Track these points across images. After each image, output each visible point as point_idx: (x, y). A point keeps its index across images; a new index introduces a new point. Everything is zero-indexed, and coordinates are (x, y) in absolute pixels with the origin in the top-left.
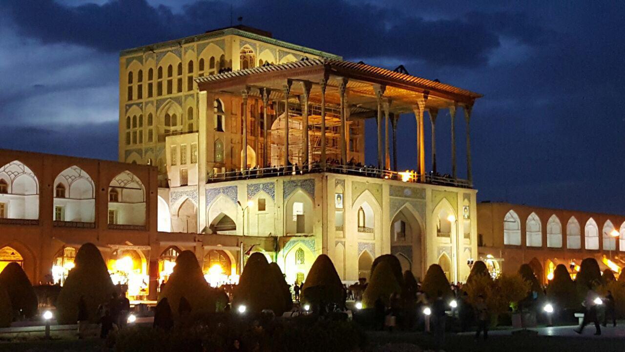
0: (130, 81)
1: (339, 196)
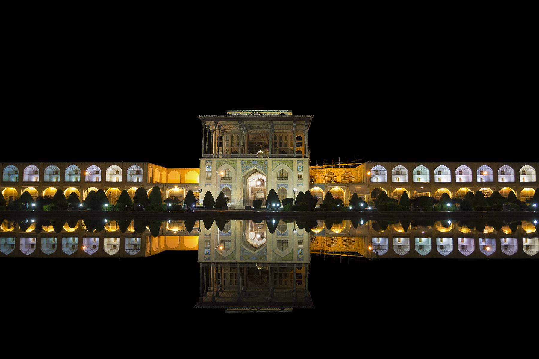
1: (209, 167)
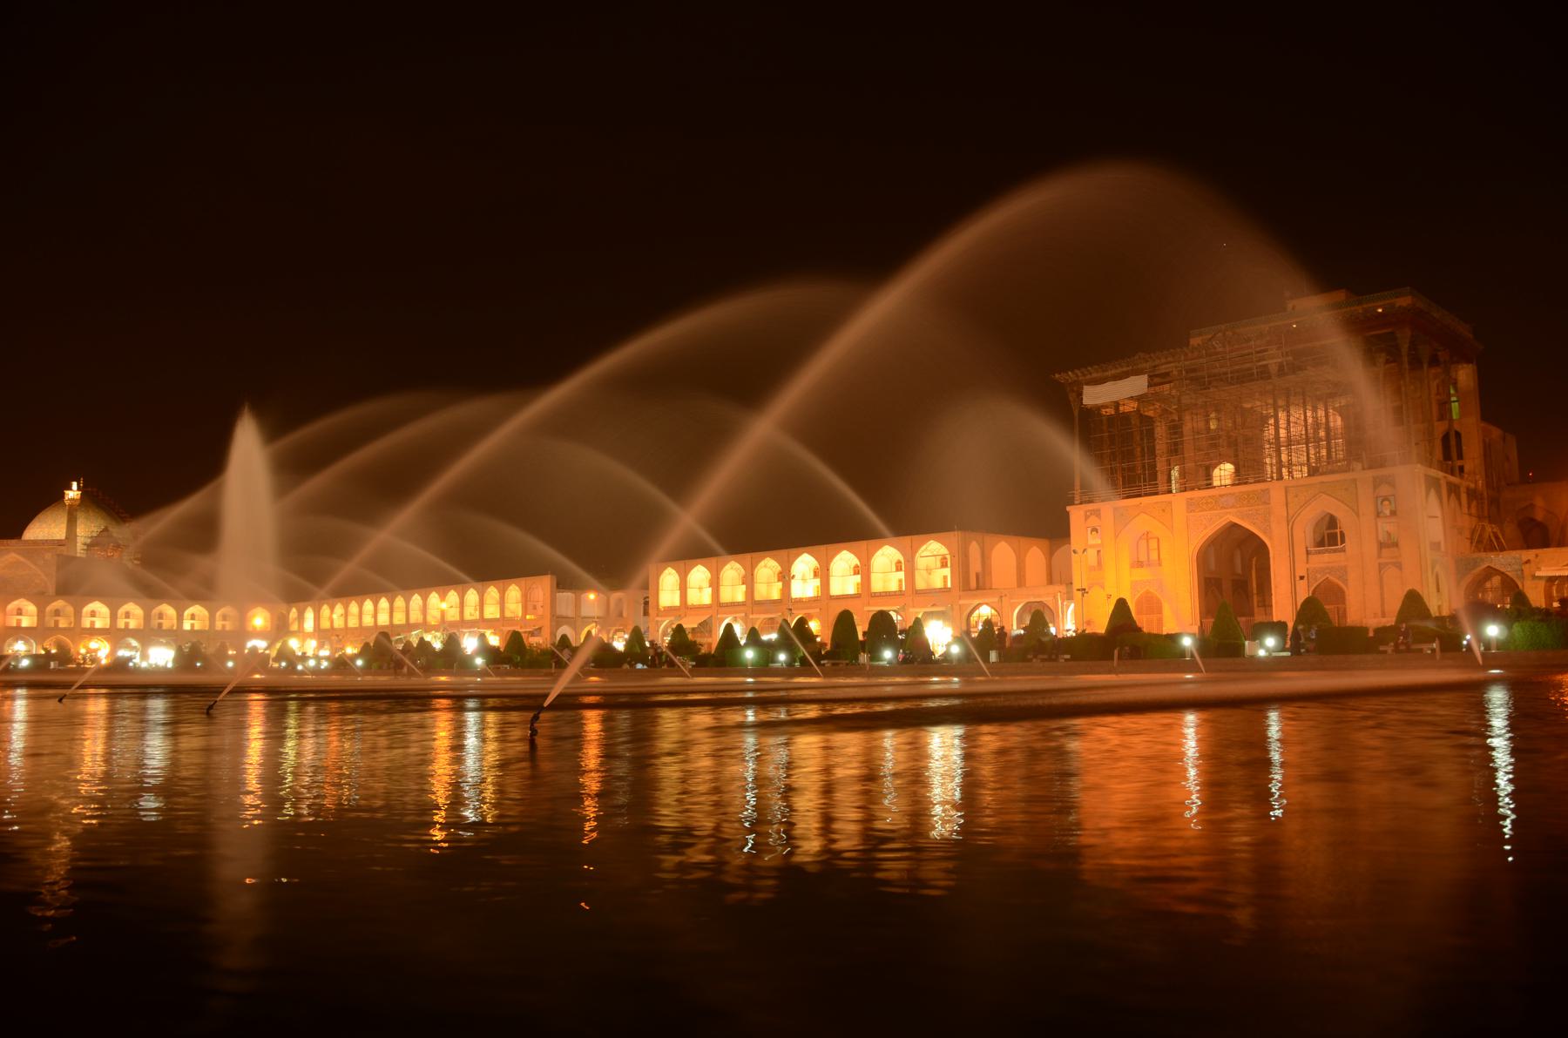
1: (1095, 530)
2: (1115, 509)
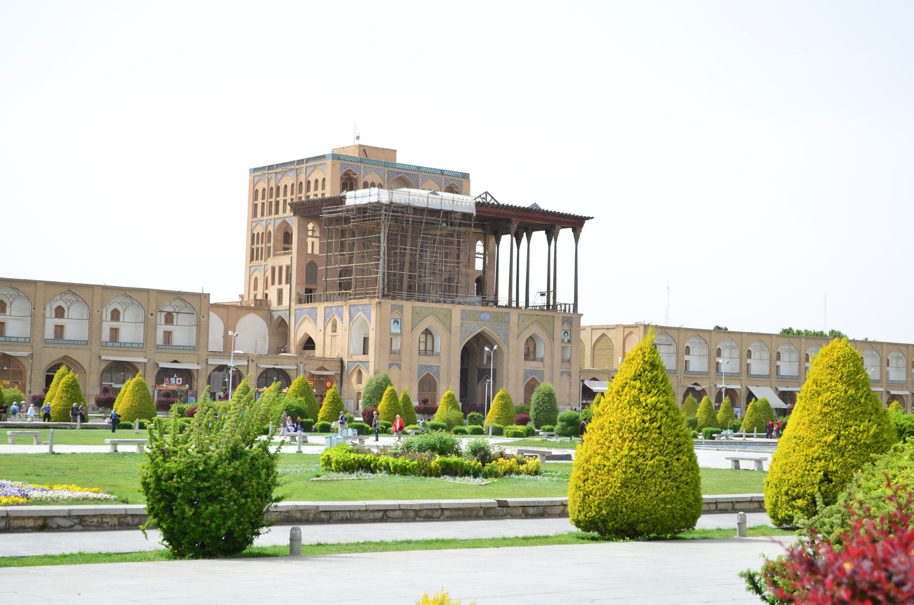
0: (256, 199)
1: (396, 321)
2: (413, 307)
